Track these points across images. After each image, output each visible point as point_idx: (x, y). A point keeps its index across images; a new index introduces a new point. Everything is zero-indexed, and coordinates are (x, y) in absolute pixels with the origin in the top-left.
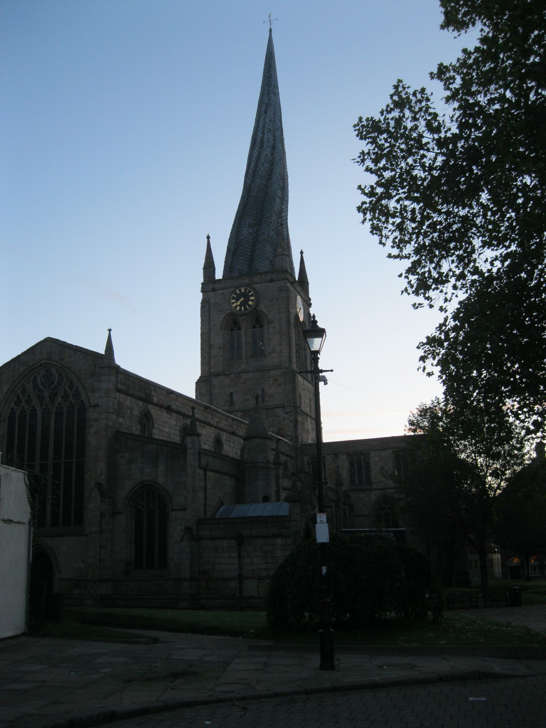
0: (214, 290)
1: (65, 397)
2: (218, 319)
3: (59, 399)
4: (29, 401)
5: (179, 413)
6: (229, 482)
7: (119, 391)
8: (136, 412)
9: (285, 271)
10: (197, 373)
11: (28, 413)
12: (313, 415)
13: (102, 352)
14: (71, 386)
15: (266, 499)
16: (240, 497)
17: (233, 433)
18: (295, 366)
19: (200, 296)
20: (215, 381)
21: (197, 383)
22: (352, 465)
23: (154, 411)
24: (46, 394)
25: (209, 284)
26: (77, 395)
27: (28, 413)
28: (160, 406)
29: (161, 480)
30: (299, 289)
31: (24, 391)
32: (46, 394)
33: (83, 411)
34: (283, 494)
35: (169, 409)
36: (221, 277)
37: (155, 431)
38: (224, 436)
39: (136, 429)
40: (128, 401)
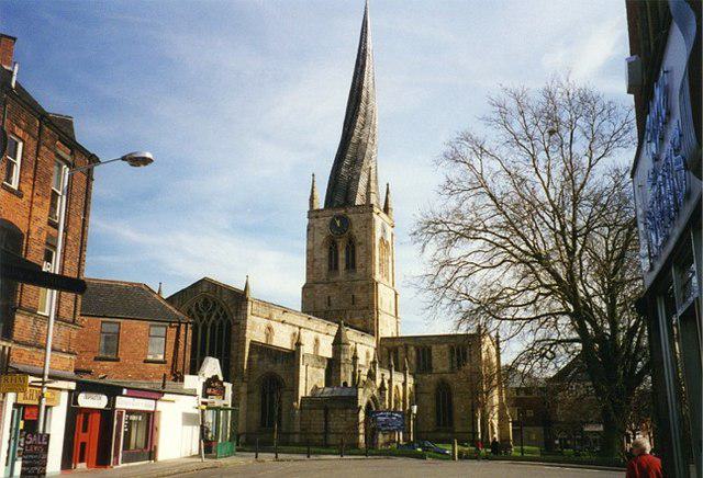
0: (317, 217)
1: (218, 317)
2: (321, 238)
8: (263, 328)
9: (372, 206)
10: (304, 282)
12: (393, 313)
19: (306, 221)
20: (317, 287)
21: (303, 288)
23: (274, 325)
24: (205, 315)
25: (313, 214)
26: (225, 316)
28: (279, 321)
29: (278, 372)
30: (383, 215)
32: (205, 315)
33: (229, 326)
36: (322, 207)
38: (321, 336)
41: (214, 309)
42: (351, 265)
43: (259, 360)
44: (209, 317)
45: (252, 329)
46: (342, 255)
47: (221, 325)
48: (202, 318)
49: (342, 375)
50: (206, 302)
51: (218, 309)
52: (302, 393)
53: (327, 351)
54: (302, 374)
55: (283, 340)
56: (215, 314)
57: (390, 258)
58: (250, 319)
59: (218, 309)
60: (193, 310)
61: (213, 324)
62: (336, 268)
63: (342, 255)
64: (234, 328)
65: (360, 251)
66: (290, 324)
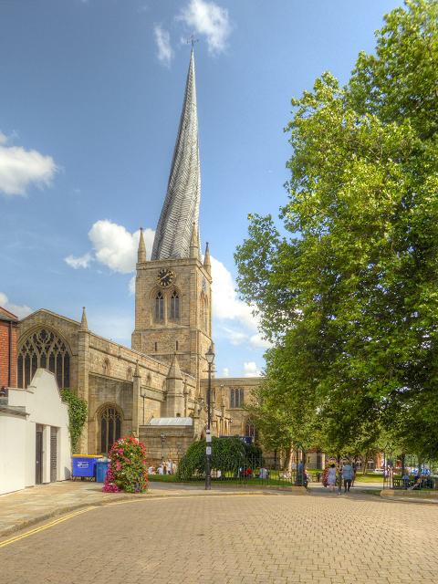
1: (56, 348)
3: (51, 349)
4: (31, 350)
5: (126, 360)
6: (158, 405)
7: (90, 347)
11: (31, 357)
13: (79, 320)
14: (59, 342)
15: (179, 415)
16: (163, 414)
17: (158, 372)
18: (199, 327)
22: (232, 393)
23: (111, 359)
24: (43, 346)
26: (63, 348)
27: (31, 357)
31: (27, 343)
32: (43, 346)
33: (67, 358)
34: (189, 412)
35: (119, 358)
37: (111, 371)
38: (153, 374)
39: (101, 370)
40: (96, 353)
41: (52, 340)
42: (175, 316)
43: (99, 390)
44: (47, 349)
45: (90, 361)
46: (167, 305)
47: (60, 355)
48: (40, 349)
49: (176, 406)
50: (43, 334)
51: (56, 341)
52: (140, 422)
53: (157, 382)
54: (140, 405)
55: (119, 371)
56: (53, 346)
57: (208, 311)
58: (88, 352)
59: (56, 341)
60: (32, 341)
61: (52, 355)
62: (162, 318)
63: (167, 305)
64: (73, 360)
65: (183, 301)
66: (126, 360)
